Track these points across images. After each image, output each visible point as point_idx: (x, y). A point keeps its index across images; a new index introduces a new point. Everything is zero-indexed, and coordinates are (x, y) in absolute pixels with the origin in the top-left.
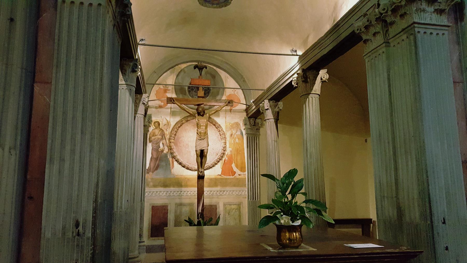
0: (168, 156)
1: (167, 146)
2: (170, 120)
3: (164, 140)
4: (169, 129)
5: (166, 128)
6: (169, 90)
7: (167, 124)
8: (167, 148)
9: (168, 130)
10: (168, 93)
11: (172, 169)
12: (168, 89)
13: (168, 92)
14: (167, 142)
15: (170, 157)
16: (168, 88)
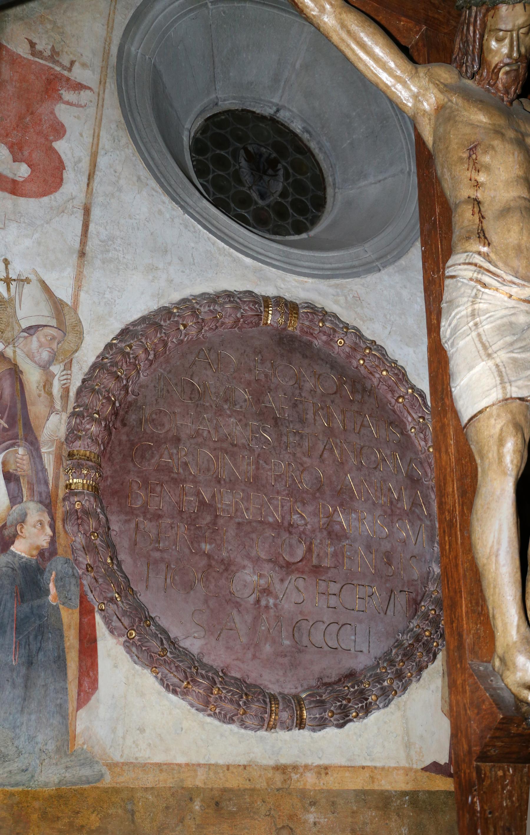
0: (47, 592)
1: (41, 502)
2: (76, 297)
3: (21, 451)
4: (68, 366)
5: (45, 355)
6: (79, 87)
7: (54, 323)
8: (46, 519)
9: (56, 369)
10: (68, 103)
11: (79, 707)
12: (68, 79)
13: (68, 95)
14: (44, 470)
15: (66, 601)
16: (70, 70)
